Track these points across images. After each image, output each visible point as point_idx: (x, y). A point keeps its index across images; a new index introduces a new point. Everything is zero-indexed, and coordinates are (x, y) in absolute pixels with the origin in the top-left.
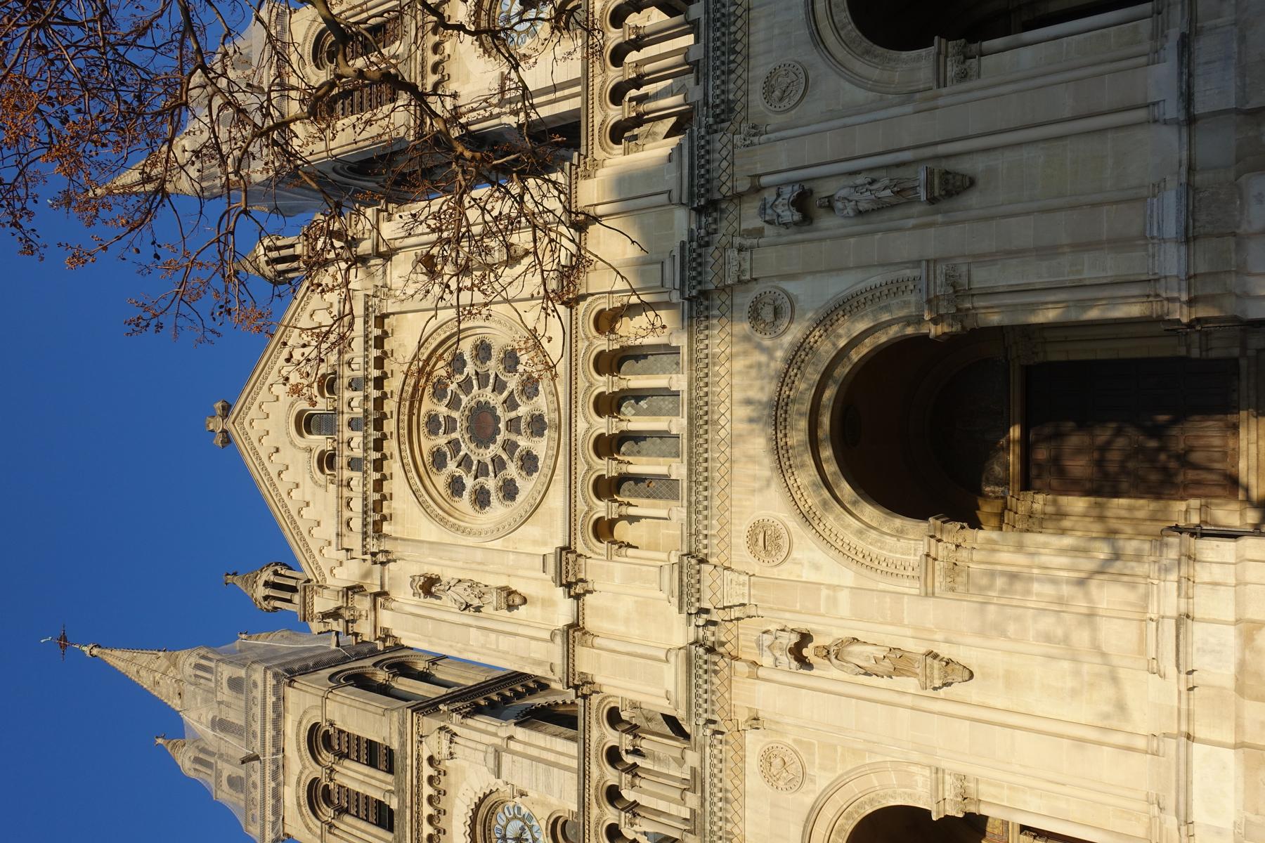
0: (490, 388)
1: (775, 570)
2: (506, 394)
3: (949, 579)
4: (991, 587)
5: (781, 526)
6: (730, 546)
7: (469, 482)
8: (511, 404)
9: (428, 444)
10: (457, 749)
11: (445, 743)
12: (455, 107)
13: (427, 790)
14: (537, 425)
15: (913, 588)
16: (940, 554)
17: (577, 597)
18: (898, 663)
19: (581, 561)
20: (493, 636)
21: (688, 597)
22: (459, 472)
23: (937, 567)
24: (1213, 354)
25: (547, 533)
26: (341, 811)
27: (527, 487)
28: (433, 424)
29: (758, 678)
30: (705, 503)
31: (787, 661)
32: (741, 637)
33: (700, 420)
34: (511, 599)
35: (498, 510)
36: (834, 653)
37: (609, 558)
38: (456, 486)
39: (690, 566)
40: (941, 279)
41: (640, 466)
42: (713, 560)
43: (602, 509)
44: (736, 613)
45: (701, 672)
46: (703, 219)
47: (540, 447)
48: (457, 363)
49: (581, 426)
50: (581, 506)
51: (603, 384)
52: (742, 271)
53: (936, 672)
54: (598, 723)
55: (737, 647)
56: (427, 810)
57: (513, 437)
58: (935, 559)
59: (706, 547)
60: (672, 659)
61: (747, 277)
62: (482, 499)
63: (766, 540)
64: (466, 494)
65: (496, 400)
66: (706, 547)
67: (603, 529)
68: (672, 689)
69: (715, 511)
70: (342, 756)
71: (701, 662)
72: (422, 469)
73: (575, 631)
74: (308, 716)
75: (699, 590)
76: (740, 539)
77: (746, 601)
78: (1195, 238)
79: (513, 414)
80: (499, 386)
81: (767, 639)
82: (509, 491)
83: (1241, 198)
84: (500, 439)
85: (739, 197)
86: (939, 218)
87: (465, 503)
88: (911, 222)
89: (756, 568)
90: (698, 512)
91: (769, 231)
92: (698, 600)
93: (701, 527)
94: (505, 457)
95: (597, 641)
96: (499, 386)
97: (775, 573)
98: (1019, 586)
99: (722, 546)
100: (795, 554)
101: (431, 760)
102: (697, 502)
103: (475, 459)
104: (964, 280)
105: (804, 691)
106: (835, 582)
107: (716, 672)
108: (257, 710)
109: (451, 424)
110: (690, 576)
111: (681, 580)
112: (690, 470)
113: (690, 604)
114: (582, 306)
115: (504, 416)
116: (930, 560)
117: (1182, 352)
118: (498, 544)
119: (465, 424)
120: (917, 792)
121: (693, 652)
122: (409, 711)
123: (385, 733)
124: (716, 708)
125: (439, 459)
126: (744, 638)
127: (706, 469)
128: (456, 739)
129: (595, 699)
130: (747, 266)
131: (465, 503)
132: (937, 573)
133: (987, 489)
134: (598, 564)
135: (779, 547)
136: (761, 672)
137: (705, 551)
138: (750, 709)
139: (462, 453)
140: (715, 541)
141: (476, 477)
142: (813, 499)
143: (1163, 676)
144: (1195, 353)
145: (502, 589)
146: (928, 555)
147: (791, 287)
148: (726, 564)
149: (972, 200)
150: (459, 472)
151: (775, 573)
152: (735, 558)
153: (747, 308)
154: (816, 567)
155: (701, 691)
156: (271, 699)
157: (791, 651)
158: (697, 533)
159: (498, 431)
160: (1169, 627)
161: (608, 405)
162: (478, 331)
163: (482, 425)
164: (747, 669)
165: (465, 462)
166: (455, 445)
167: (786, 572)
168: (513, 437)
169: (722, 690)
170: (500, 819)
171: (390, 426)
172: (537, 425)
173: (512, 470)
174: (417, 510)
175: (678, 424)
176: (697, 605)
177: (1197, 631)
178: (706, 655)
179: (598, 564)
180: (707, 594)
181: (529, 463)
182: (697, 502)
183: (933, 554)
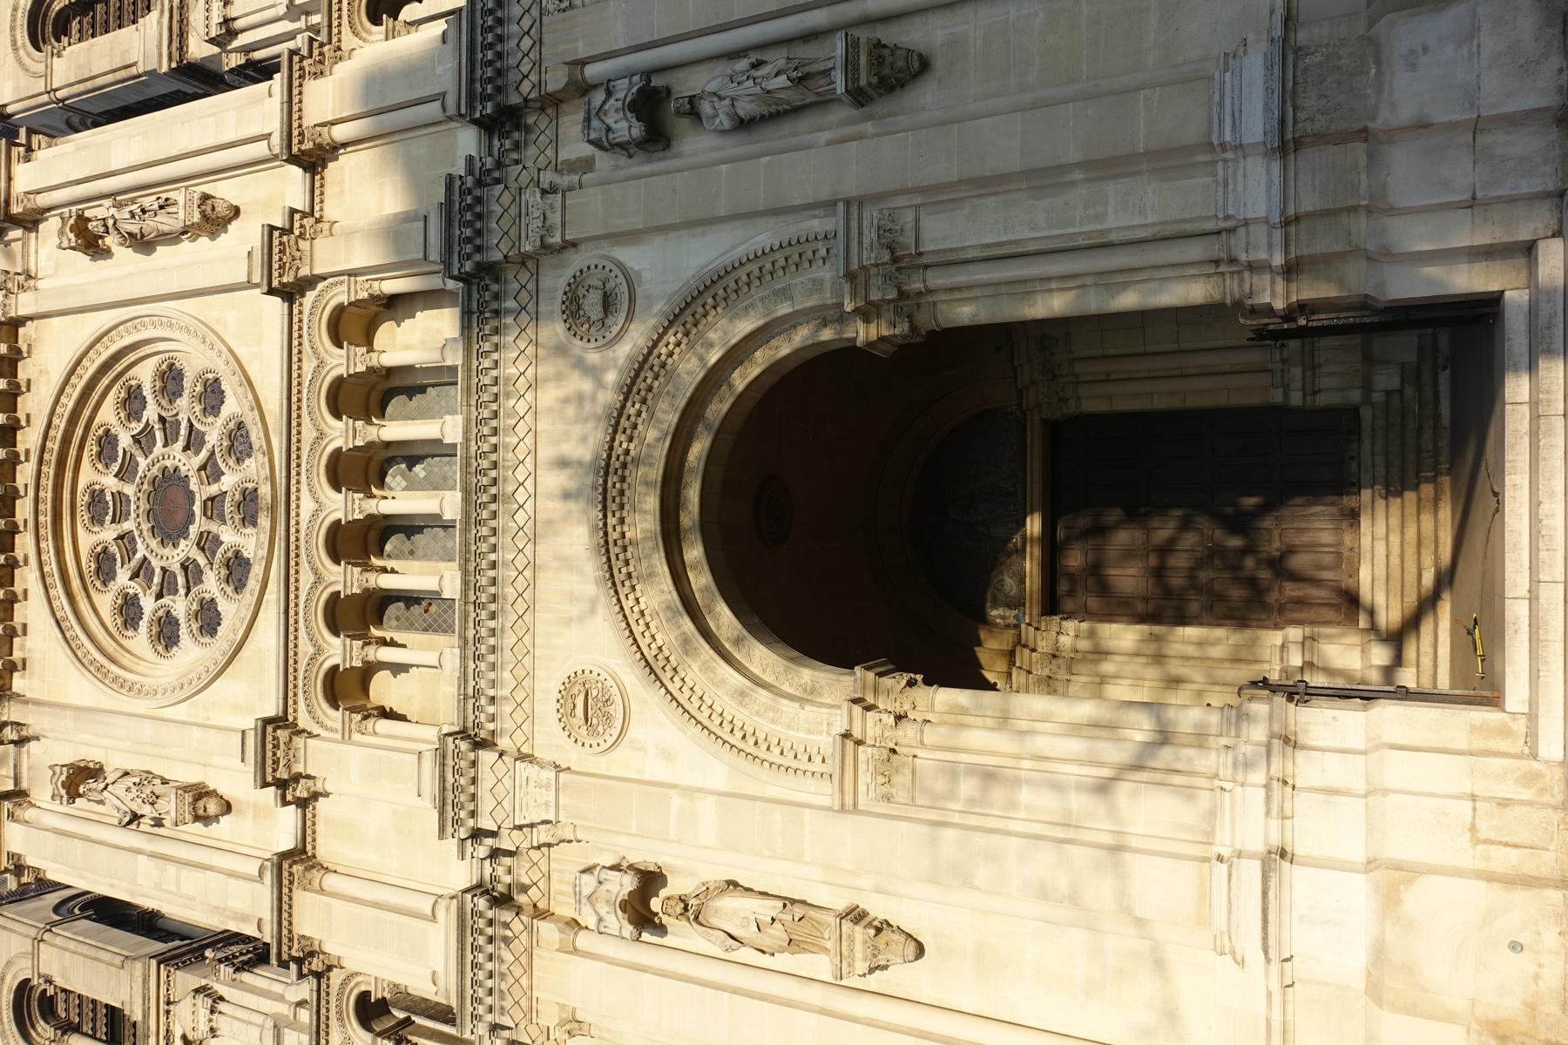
0: (181, 443)
1: (603, 759)
2: (204, 454)
3: (881, 779)
4: (951, 795)
5: (610, 682)
6: (531, 717)
7: (148, 604)
8: (211, 470)
10: (221, 1022)
11: (203, 1013)
12: (227, 21)
15: (824, 793)
16: (870, 732)
17: (302, 804)
19: (299, 741)
20: (171, 869)
21: (455, 807)
22: (134, 588)
23: (862, 757)
24: (1324, 400)
25: (252, 691)
27: (232, 611)
29: (575, 951)
30: (492, 641)
31: (618, 923)
32: (554, 876)
33: (484, 494)
34: (203, 803)
35: (192, 653)
36: (693, 912)
37: (346, 737)
38: (129, 610)
39: (458, 754)
40: (870, 235)
42: (503, 742)
43: (338, 651)
44: (542, 835)
45: (481, 940)
46: (496, 143)
49: (307, 506)
50: (305, 648)
52: (547, 229)
53: (858, 947)
54: (341, 1019)
55: (548, 894)
57: (214, 527)
58: (859, 743)
59: (492, 718)
60: (441, 914)
61: (556, 239)
62: (166, 633)
63: (587, 706)
64: (143, 624)
65: (189, 464)
66: (492, 718)
68: (440, 969)
69: (507, 654)
71: (481, 923)
72: (76, 583)
73: (295, 864)
74: (14, 969)
75: (473, 797)
76: (546, 707)
77: (551, 817)
78: (1298, 144)
79: (213, 489)
80: (194, 442)
81: (589, 882)
82: (208, 618)
83: (1378, 63)
84: (193, 530)
85: (552, 102)
86: (869, 127)
87: (140, 640)
88: (825, 136)
89: (570, 755)
90: (478, 658)
91: (603, 161)
92: (473, 814)
93: (483, 684)
94: (202, 561)
95: (330, 881)
96: (194, 442)
97: (603, 764)
98: (998, 794)
99: (519, 716)
100: (633, 732)
102: (478, 640)
103: (156, 564)
104: (909, 238)
105: (646, 976)
106: (697, 782)
107: (506, 940)
110: (458, 771)
111: (443, 779)
112: (465, 583)
113: (457, 822)
114: (310, 296)
115: (202, 491)
116: (850, 744)
117: (1277, 397)
118: (180, 712)
119: (144, 506)
121: (469, 906)
122: (154, 962)
124: (508, 1003)
125: (104, 566)
126: (557, 879)
127: (494, 582)
128: (221, 1006)
129: (336, 977)
130: (555, 219)
131: (140, 640)
132: (862, 767)
133: (994, 613)
135: (608, 718)
136: (583, 941)
137: (491, 726)
138: (562, 1006)
139: (139, 556)
140: (508, 709)
141: (159, 596)
142: (669, 632)
143: (1241, 963)
144: (1296, 399)
145: (186, 789)
146: (846, 735)
147: (629, 256)
148: (525, 750)
149: (926, 96)
150: (134, 588)
151: (603, 764)
152: (539, 739)
153: (560, 296)
154: (668, 756)
155: (481, 975)
157: (625, 906)
158: (478, 692)
159: (190, 519)
160: (1251, 872)
161: (359, 469)
162: (161, 346)
163: (169, 506)
164: (557, 936)
165: (142, 571)
167: (619, 762)
168: (214, 527)
169: (517, 971)
171: (24, 510)
173: (211, 583)
174: (61, 653)
175: (449, 504)
176: (471, 823)
177: (1297, 879)
179: (332, 752)
180: (486, 804)
182: (478, 640)
183: (857, 734)
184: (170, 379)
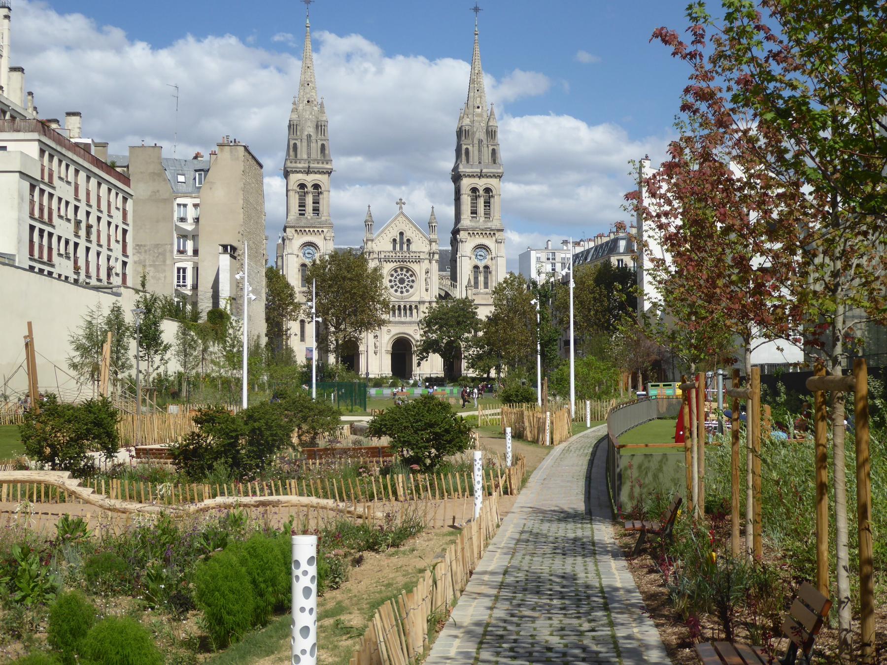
10: (328, 242)
13: (316, 230)
14: (402, 292)
47: (398, 294)
48: (411, 276)
51: (408, 306)
56: (311, 230)
63: (389, 331)
108: (320, 165)
161: (405, 306)
163: (402, 281)
181: (396, 291)
184: (413, 281)
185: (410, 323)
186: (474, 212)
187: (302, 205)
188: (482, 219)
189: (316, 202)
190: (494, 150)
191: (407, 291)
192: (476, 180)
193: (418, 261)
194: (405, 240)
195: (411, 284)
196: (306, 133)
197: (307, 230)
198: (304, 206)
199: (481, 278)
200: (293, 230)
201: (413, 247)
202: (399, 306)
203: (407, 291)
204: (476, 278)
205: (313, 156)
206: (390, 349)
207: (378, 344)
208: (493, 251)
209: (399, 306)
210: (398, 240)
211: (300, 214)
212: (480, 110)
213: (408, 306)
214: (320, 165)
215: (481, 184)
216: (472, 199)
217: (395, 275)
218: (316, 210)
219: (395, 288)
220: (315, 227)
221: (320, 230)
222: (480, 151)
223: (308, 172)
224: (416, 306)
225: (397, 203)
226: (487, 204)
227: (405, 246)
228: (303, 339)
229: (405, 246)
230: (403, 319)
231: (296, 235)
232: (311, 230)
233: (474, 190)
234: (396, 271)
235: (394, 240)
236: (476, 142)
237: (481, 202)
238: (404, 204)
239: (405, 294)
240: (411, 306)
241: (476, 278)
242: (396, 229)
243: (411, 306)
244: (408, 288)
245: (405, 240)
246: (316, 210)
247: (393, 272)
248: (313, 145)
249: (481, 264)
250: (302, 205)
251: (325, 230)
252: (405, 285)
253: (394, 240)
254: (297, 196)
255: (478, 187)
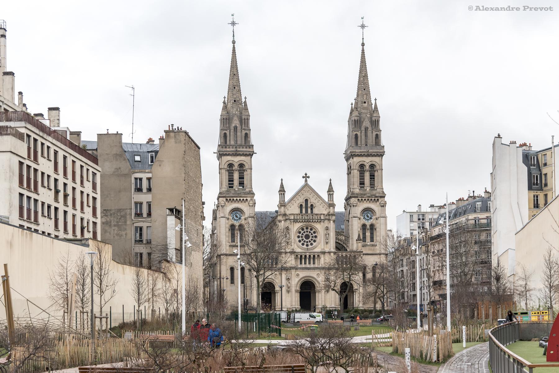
9: (305, 228)
13: (242, 199)
14: (307, 245)
18: (289, 288)
26: (228, 170)
27: (300, 244)
28: (307, 228)
35: (297, 240)
41: (303, 260)
43: (299, 256)
47: (305, 246)
48: (314, 232)
51: (312, 256)
56: (238, 199)
63: (298, 275)
67: (297, 256)
70: (239, 171)
73: (286, 253)
80: (312, 240)
101: (247, 200)
109: (307, 232)
120: (277, 288)
123: (248, 187)
134: (293, 257)
156: (248, 153)
161: (310, 256)
163: (307, 237)
166: (304, 232)
170: (239, 213)
172: (307, 245)
178: (287, 269)
179: (293, 257)
181: (303, 244)
185: (314, 269)
186: (362, 183)
187: (231, 180)
188: (368, 189)
189: (241, 178)
190: (377, 135)
191: (312, 244)
192: (364, 159)
193: (320, 221)
194: (309, 205)
195: (314, 239)
196: (233, 125)
197: (235, 199)
198: (233, 181)
199: (368, 234)
200: (224, 199)
201: (316, 211)
202: (305, 256)
203: (312, 244)
204: (364, 234)
205: (239, 142)
206: (298, 288)
207: (289, 285)
208: (377, 213)
209: (305, 256)
210: (304, 205)
211: (230, 187)
212: (366, 104)
213: (312, 256)
214: (244, 149)
215: (367, 161)
216: (360, 173)
217: (302, 232)
218: (241, 184)
219: (302, 242)
220: (241, 197)
221: (245, 199)
222: (366, 136)
223: (236, 154)
224: (318, 256)
225: (303, 177)
226: (372, 177)
227: (309, 210)
228: (232, 281)
229: (309, 210)
230: (308, 265)
231: (227, 203)
232: (238, 199)
233: (362, 166)
234: (303, 229)
235: (301, 205)
236: (363, 129)
237: (367, 176)
238: (309, 177)
239: (310, 247)
240: (314, 256)
241: (364, 234)
242: (302, 197)
243: (314, 256)
244: (312, 242)
245: (309, 205)
246: (241, 184)
247: (301, 230)
248: (239, 134)
249: (368, 223)
250: (231, 180)
251: (249, 199)
252: (310, 239)
253: (301, 205)
254: (227, 173)
255: (365, 163)
